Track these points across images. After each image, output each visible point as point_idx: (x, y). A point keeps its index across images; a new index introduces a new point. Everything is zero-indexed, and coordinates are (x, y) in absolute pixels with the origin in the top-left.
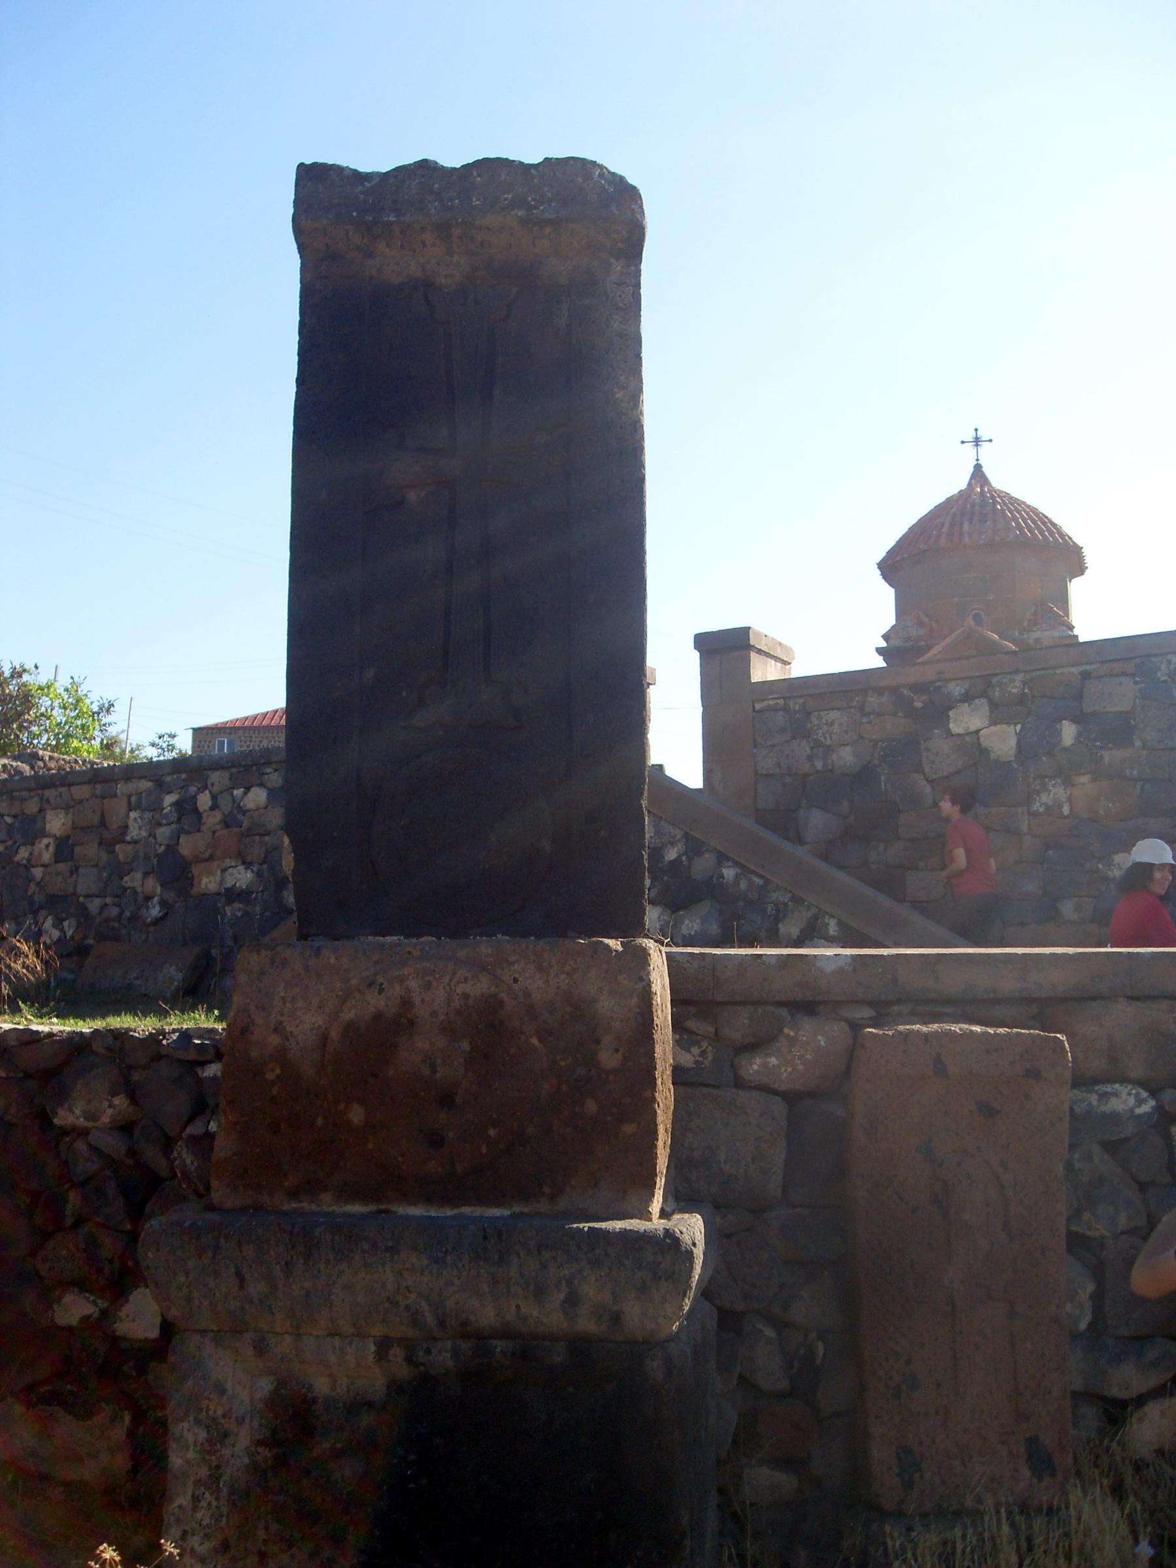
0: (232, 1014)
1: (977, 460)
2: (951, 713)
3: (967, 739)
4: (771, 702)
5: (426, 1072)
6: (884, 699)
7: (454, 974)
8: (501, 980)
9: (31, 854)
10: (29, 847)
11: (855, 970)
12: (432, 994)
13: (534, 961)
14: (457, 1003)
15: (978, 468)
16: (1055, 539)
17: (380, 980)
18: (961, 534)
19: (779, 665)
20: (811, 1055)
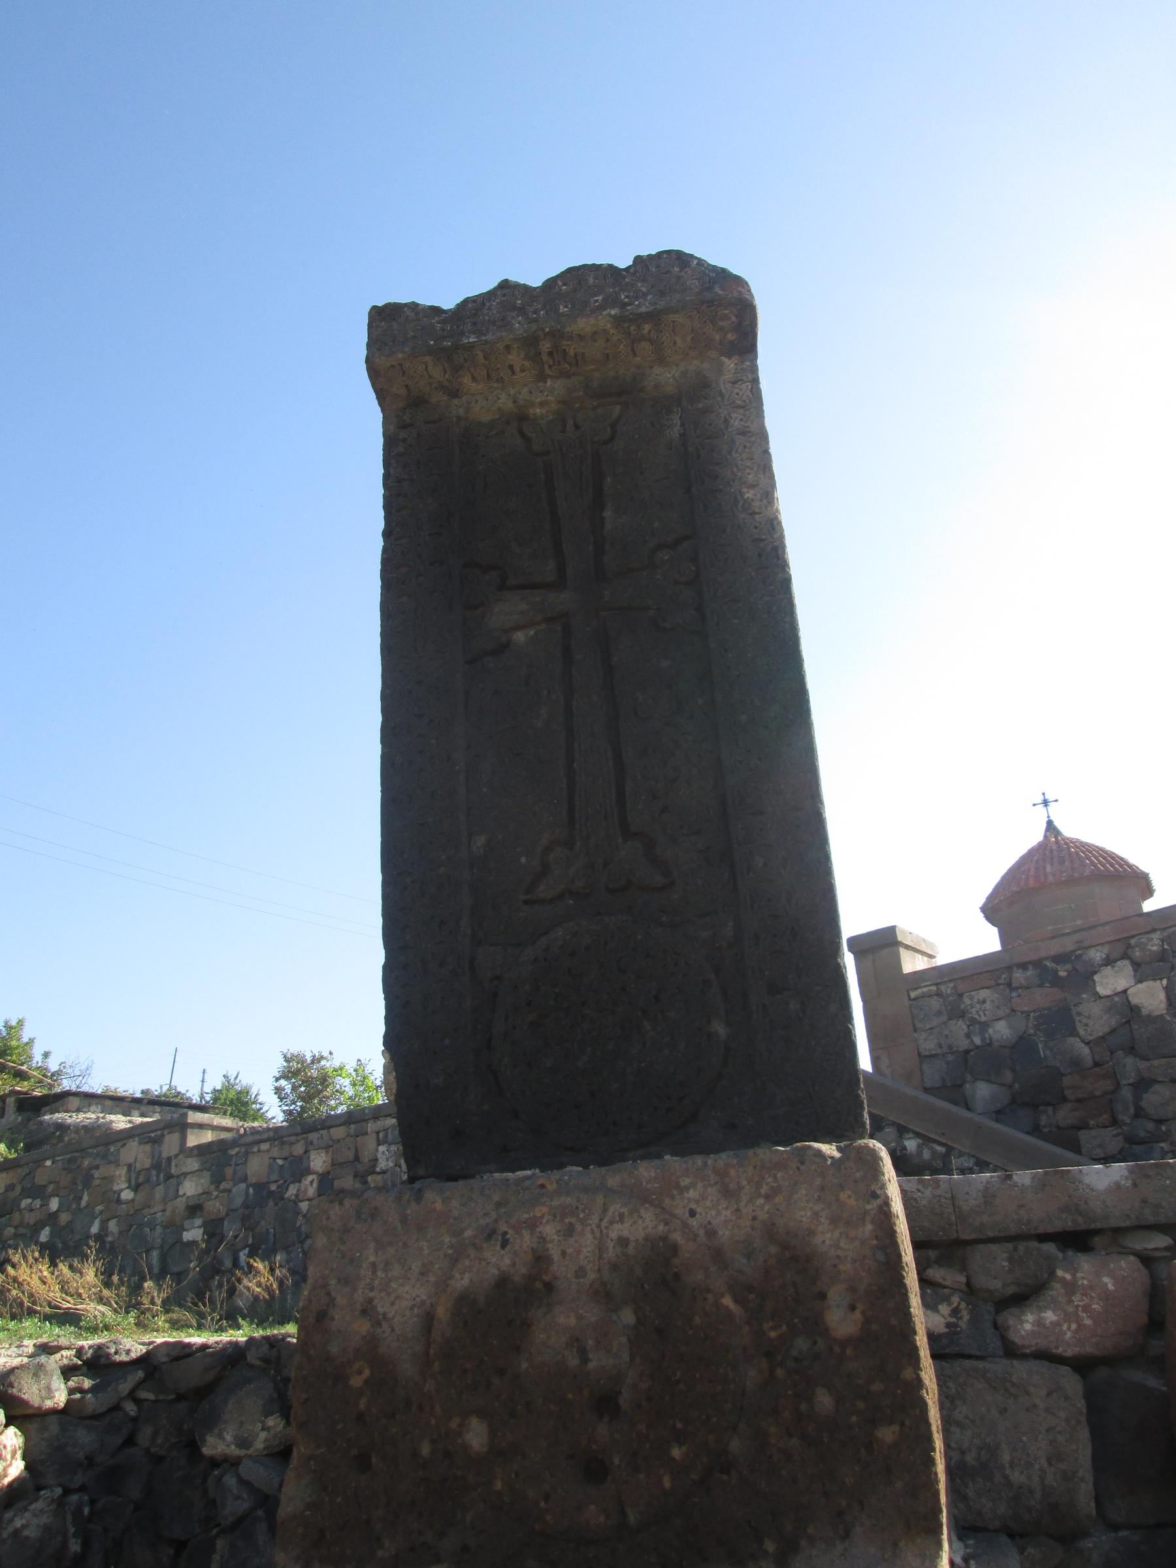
0: (306, 1293)
1: (1048, 817)
2: (1096, 978)
3: (1116, 999)
4: (925, 990)
5: (573, 1362)
6: (1030, 973)
7: (605, 1210)
8: (673, 1216)
9: (298, 1190)
10: (297, 1184)
11: (1135, 1185)
12: (576, 1241)
13: (716, 1183)
14: (611, 1252)
15: (1050, 824)
16: (1125, 870)
17: (503, 1227)
18: (1045, 875)
19: (926, 959)
20: (1099, 1304)
